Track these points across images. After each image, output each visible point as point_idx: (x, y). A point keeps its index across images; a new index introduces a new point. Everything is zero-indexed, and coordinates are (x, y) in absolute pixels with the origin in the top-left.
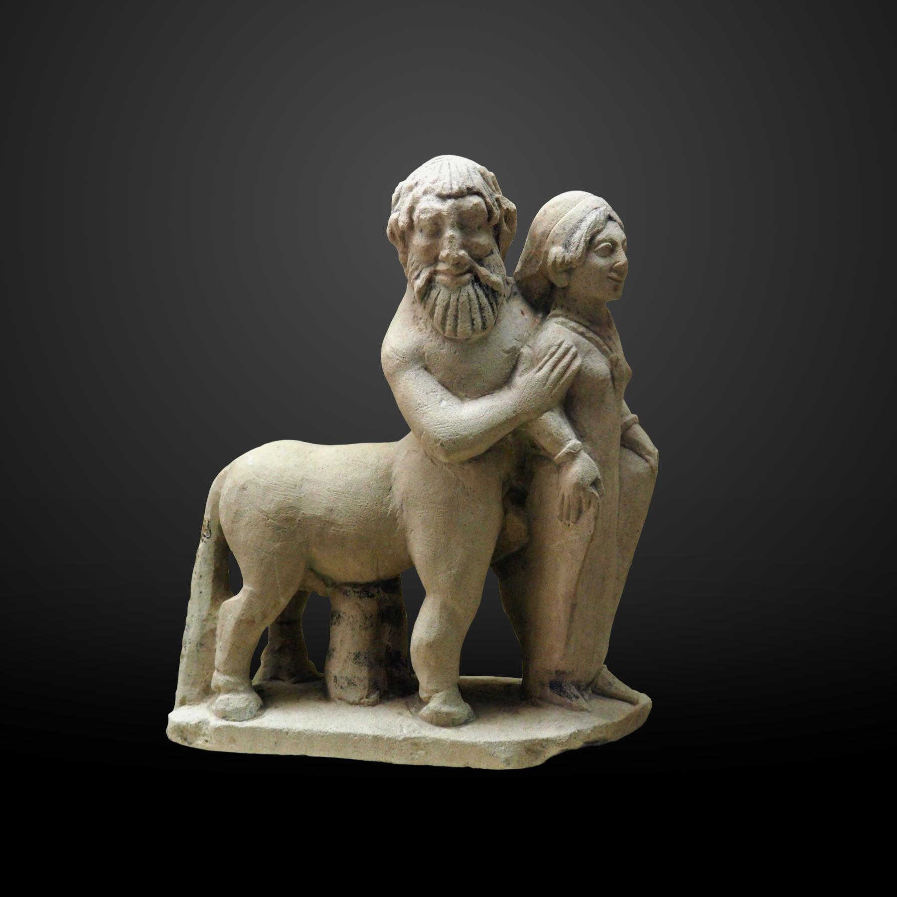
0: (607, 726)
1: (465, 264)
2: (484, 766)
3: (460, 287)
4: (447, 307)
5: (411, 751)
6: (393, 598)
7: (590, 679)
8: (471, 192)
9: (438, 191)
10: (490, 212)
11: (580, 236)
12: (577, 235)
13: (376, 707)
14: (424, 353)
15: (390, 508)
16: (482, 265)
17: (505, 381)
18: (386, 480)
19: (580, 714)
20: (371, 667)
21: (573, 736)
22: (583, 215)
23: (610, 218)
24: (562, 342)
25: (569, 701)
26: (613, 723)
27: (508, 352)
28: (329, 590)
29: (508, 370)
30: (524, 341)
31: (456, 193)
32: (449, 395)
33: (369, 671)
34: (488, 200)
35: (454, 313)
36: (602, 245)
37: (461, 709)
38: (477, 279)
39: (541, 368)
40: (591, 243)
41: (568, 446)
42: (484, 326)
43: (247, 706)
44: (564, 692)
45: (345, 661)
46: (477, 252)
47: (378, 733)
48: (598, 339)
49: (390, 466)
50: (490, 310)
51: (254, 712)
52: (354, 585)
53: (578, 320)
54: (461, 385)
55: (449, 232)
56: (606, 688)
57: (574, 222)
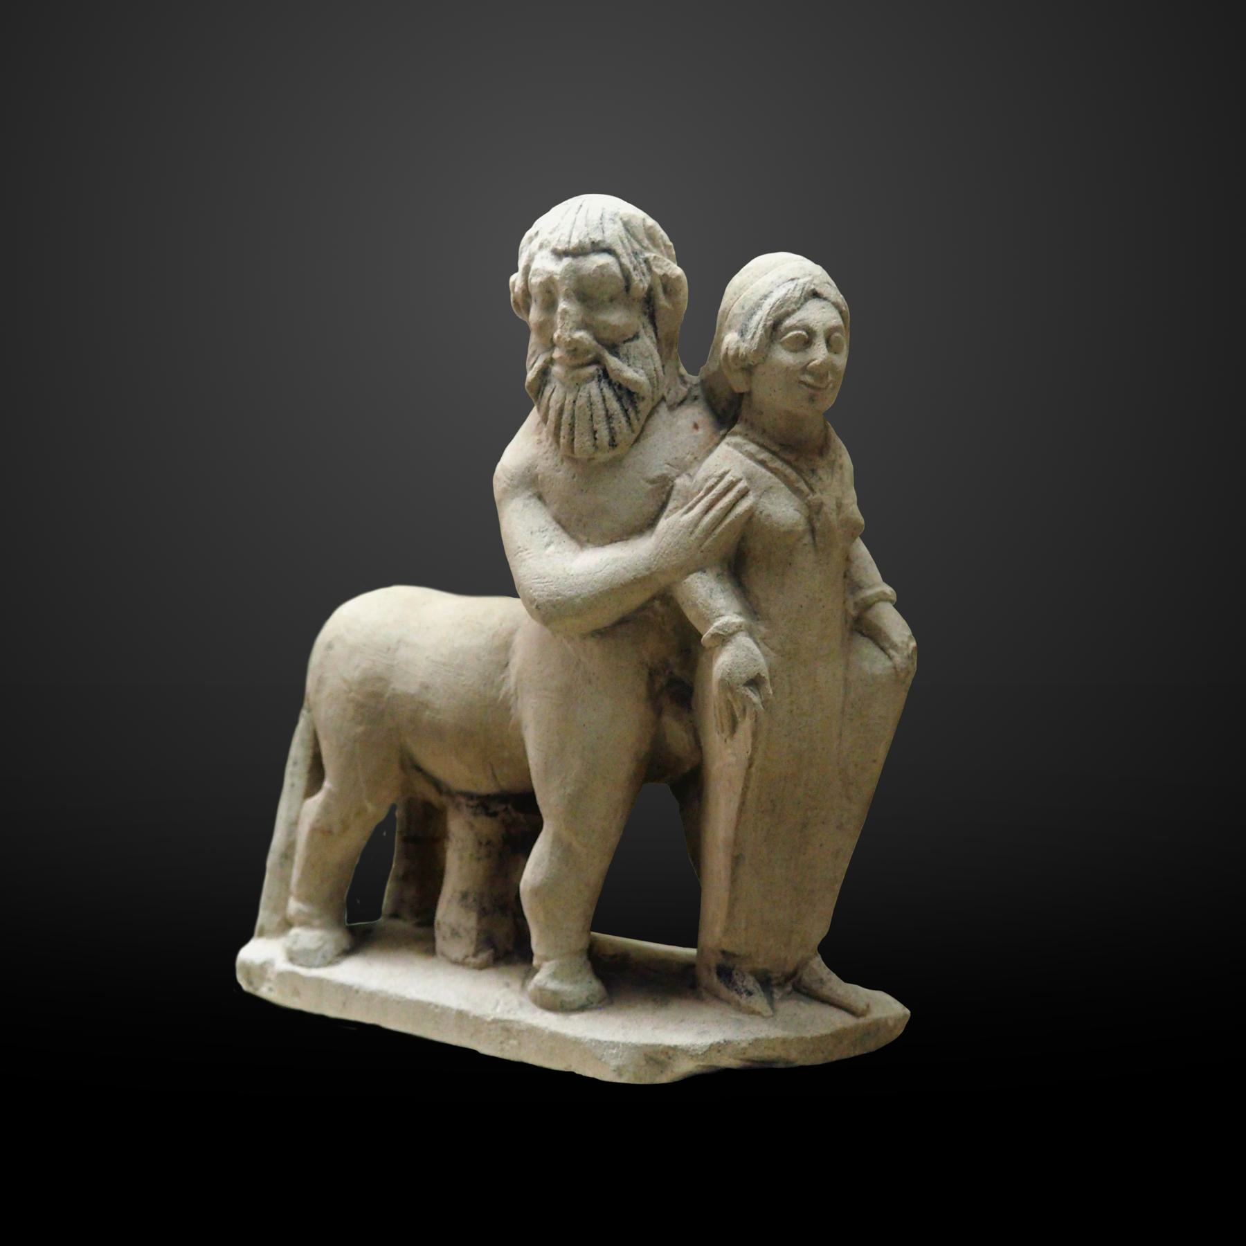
0: (784, 1041)
1: (588, 352)
2: (589, 1073)
3: (579, 384)
4: (561, 411)
5: (501, 1039)
6: (513, 818)
7: (789, 969)
8: (597, 248)
9: (553, 245)
10: (627, 278)
11: (761, 317)
12: (756, 318)
13: (483, 972)
14: (537, 476)
15: (502, 693)
16: (616, 354)
17: (648, 524)
18: (502, 650)
19: (746, 1018)
20: (483, 913)
21: (717, 1048)
22: (769, 289)
23: (815, 295)
24: (725, 473)
25: (737, 997)
26: (801, 1040)
27: (652, 482)
28: (444, 799)
29: (653, 509)
30: (684, 468)
31: (574, 249)
32: (565, 537)
33: (479, 920)
34: (625, 260)
35: (569, 421)
36: (790, 334)
37: (588, 986)
38: (605, 375)
39: (691, 509)
40: (774, 329)
41: (716, 624)
42: (613, 444)
43: (320, 948)
44: (735, 984)
45: (449, 901)
46: (606, 335)
47: (465, 1006)
48: (789, 471)
49: (512, 633)
50: (623, 420)
51: (329, 957)
52: (470, 796)
53: (761, 441)
54: (581, 526)
55: (562, 305)
56: (815, 986)
57: (756, 298)
